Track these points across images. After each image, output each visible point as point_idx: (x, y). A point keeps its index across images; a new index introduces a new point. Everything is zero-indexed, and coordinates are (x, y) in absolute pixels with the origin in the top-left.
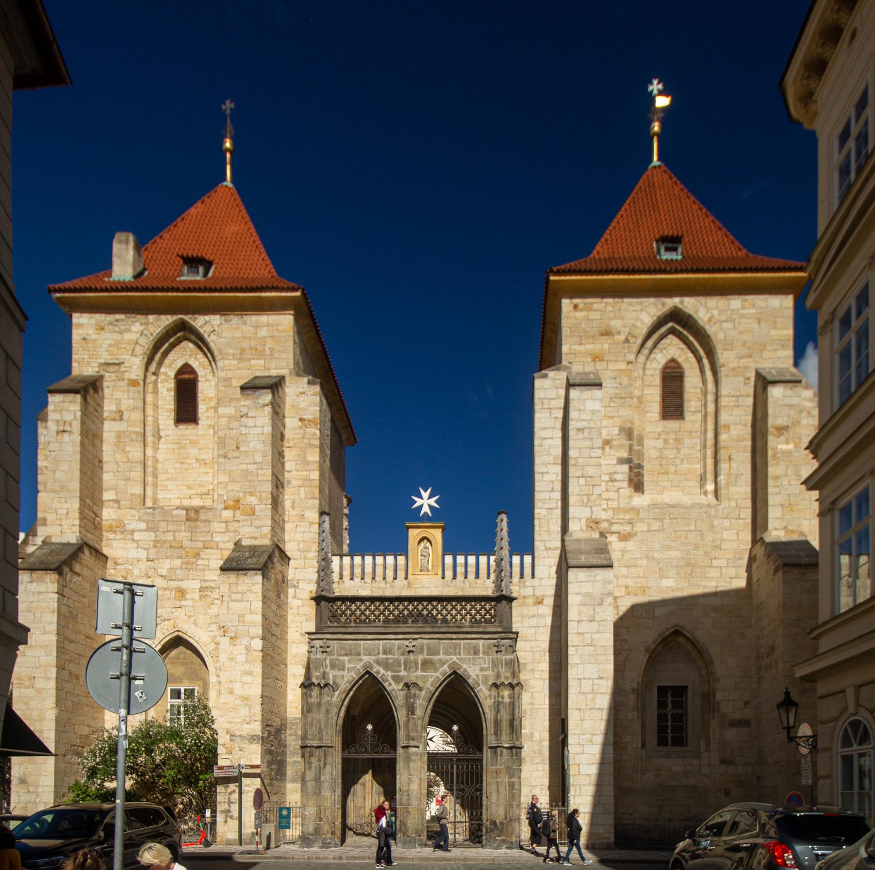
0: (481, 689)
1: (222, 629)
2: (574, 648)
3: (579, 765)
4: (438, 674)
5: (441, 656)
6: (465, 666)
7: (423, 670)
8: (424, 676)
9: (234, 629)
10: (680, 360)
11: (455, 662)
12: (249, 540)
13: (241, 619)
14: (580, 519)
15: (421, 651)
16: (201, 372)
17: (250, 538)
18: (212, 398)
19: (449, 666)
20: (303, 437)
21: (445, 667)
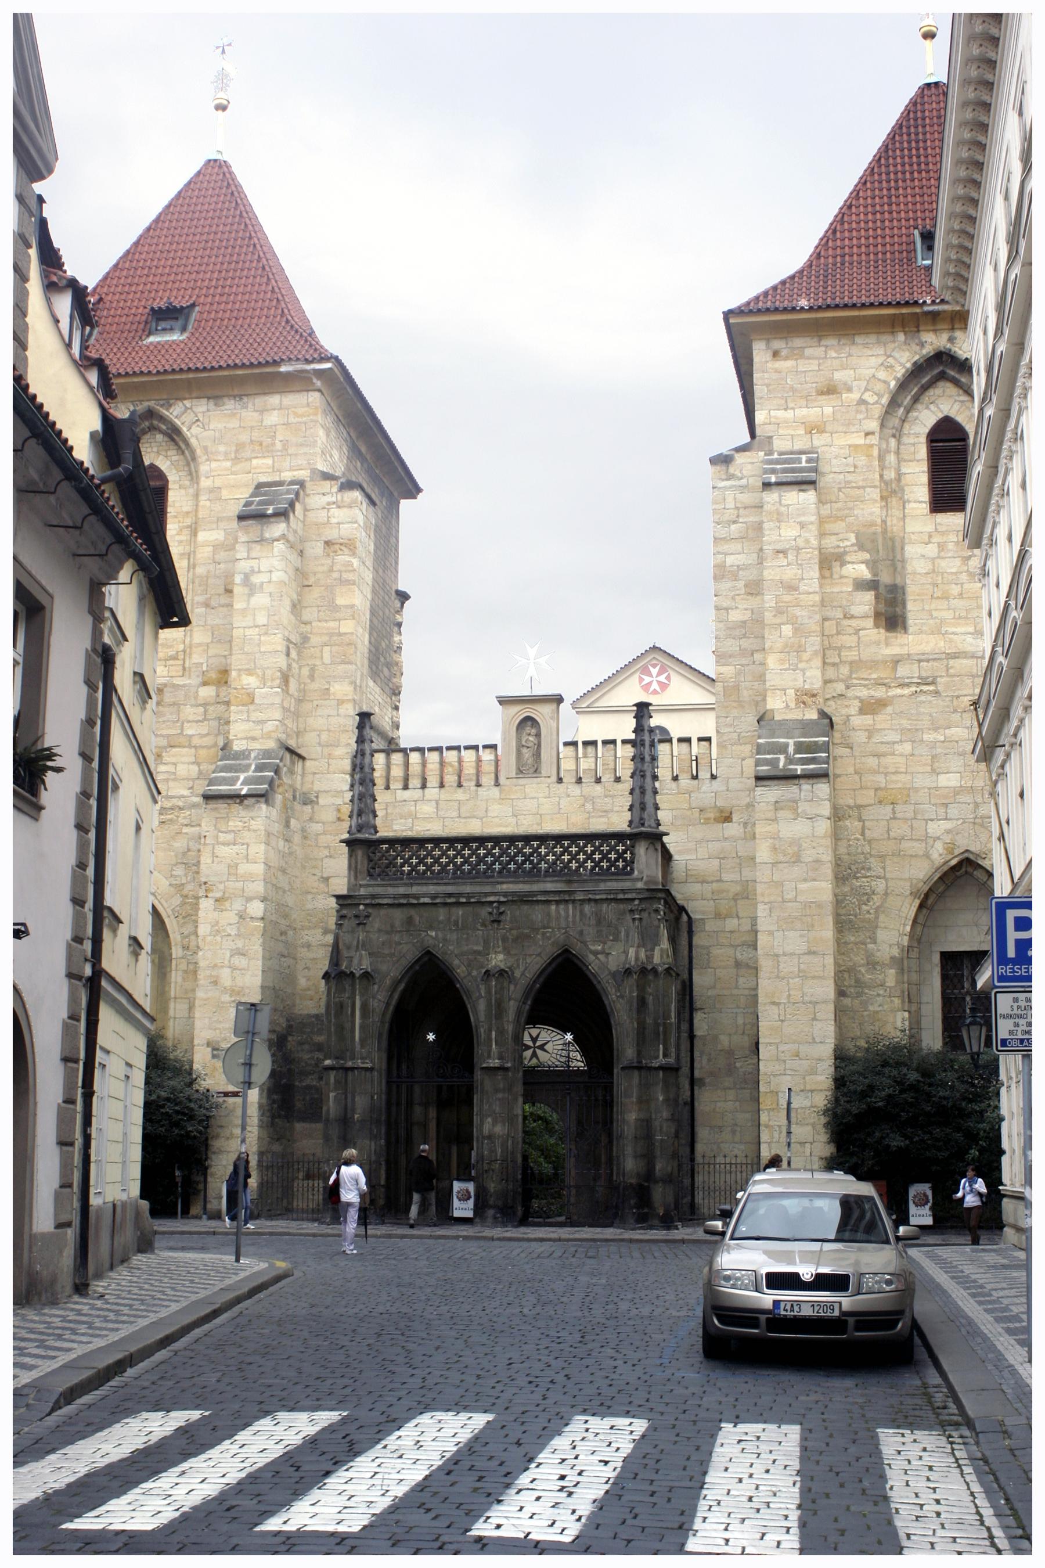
1: (203, 887)
3: (777, 1093)
9: (221, 887)
10: (959, 419)
12: (244, 742)
13: (233, 871)
14: (785, 690)
16: (172, 477)
17: (246, 738)
18: (188, 513)
20: (331, 570)
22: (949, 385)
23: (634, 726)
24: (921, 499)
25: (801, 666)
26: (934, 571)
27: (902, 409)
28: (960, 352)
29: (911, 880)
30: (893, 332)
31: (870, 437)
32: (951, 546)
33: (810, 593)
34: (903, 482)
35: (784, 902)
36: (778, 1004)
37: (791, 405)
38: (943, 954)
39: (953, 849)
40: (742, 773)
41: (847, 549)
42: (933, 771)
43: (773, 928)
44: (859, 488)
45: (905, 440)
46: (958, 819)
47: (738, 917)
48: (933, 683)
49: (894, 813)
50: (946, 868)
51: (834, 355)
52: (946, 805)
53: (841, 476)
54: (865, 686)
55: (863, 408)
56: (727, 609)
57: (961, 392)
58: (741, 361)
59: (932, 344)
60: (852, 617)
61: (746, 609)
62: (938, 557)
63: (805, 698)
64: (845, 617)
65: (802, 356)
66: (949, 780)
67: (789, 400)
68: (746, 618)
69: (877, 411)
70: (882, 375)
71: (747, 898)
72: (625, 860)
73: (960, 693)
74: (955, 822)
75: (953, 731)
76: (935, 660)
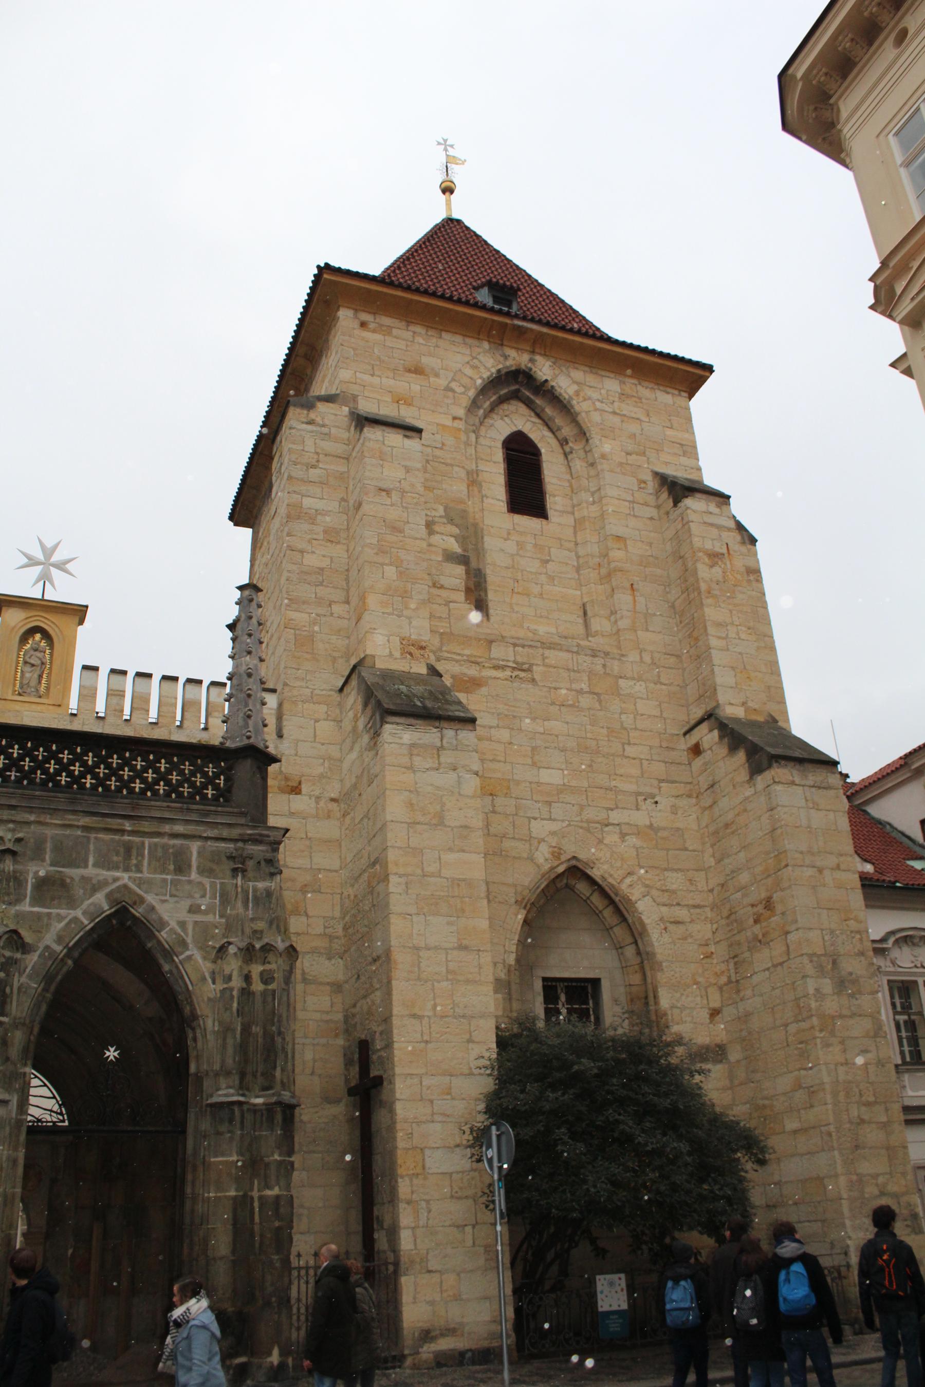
0: (189, 958)
2: (402, 880)
4: (78, 913)
6: (150, 898)
7: (36, 901)
8: (39, 916)
10: (533, 436)
11: (125, 886)
15: (38, 854)
19: (108, 896)
21: (100, 898)
23: (237, 613)
24: (498, 497)
25: (406, 613)
26: (513, 567)
27: (481, 412)
28: (540, 374)
29: (515, 886)
30: (479, 339)
31: (457, 421)
32: (529, 547)
33: (416, 539)
34: (480, 478)
35: (424, 876)
36: (419, 1017)
37: (377, 373)
38: (545, 979)
39: (560, 854)
40: (315, 736)
41: (436, 519)
42: (534, 764)
43: (412, 910)
44: (447, 464)
45: (482, 440)
46: (563, 821)
47: (307, 915)
48: (529, 670)
50: (553, 876)
51: (421, 341)
52: (549, 803)
53: (429, 450)
54: (457, 661)
55: (450, 394)
56: (302, 552)
57: (533, 414)
58: (301, 350)
59: (514, 359)
60: (442, 587)
61: (324, 556)
62: (518, 554)
63: (412, 649)
64: (434, 585)
66: (551, 777)
67: (375, 368)
68: (323, 565)
69: (465, 401)
70: (468, 371)
72: (216, 787)
74: (560, 823)
75: (553, 723)
76: (530, 646)
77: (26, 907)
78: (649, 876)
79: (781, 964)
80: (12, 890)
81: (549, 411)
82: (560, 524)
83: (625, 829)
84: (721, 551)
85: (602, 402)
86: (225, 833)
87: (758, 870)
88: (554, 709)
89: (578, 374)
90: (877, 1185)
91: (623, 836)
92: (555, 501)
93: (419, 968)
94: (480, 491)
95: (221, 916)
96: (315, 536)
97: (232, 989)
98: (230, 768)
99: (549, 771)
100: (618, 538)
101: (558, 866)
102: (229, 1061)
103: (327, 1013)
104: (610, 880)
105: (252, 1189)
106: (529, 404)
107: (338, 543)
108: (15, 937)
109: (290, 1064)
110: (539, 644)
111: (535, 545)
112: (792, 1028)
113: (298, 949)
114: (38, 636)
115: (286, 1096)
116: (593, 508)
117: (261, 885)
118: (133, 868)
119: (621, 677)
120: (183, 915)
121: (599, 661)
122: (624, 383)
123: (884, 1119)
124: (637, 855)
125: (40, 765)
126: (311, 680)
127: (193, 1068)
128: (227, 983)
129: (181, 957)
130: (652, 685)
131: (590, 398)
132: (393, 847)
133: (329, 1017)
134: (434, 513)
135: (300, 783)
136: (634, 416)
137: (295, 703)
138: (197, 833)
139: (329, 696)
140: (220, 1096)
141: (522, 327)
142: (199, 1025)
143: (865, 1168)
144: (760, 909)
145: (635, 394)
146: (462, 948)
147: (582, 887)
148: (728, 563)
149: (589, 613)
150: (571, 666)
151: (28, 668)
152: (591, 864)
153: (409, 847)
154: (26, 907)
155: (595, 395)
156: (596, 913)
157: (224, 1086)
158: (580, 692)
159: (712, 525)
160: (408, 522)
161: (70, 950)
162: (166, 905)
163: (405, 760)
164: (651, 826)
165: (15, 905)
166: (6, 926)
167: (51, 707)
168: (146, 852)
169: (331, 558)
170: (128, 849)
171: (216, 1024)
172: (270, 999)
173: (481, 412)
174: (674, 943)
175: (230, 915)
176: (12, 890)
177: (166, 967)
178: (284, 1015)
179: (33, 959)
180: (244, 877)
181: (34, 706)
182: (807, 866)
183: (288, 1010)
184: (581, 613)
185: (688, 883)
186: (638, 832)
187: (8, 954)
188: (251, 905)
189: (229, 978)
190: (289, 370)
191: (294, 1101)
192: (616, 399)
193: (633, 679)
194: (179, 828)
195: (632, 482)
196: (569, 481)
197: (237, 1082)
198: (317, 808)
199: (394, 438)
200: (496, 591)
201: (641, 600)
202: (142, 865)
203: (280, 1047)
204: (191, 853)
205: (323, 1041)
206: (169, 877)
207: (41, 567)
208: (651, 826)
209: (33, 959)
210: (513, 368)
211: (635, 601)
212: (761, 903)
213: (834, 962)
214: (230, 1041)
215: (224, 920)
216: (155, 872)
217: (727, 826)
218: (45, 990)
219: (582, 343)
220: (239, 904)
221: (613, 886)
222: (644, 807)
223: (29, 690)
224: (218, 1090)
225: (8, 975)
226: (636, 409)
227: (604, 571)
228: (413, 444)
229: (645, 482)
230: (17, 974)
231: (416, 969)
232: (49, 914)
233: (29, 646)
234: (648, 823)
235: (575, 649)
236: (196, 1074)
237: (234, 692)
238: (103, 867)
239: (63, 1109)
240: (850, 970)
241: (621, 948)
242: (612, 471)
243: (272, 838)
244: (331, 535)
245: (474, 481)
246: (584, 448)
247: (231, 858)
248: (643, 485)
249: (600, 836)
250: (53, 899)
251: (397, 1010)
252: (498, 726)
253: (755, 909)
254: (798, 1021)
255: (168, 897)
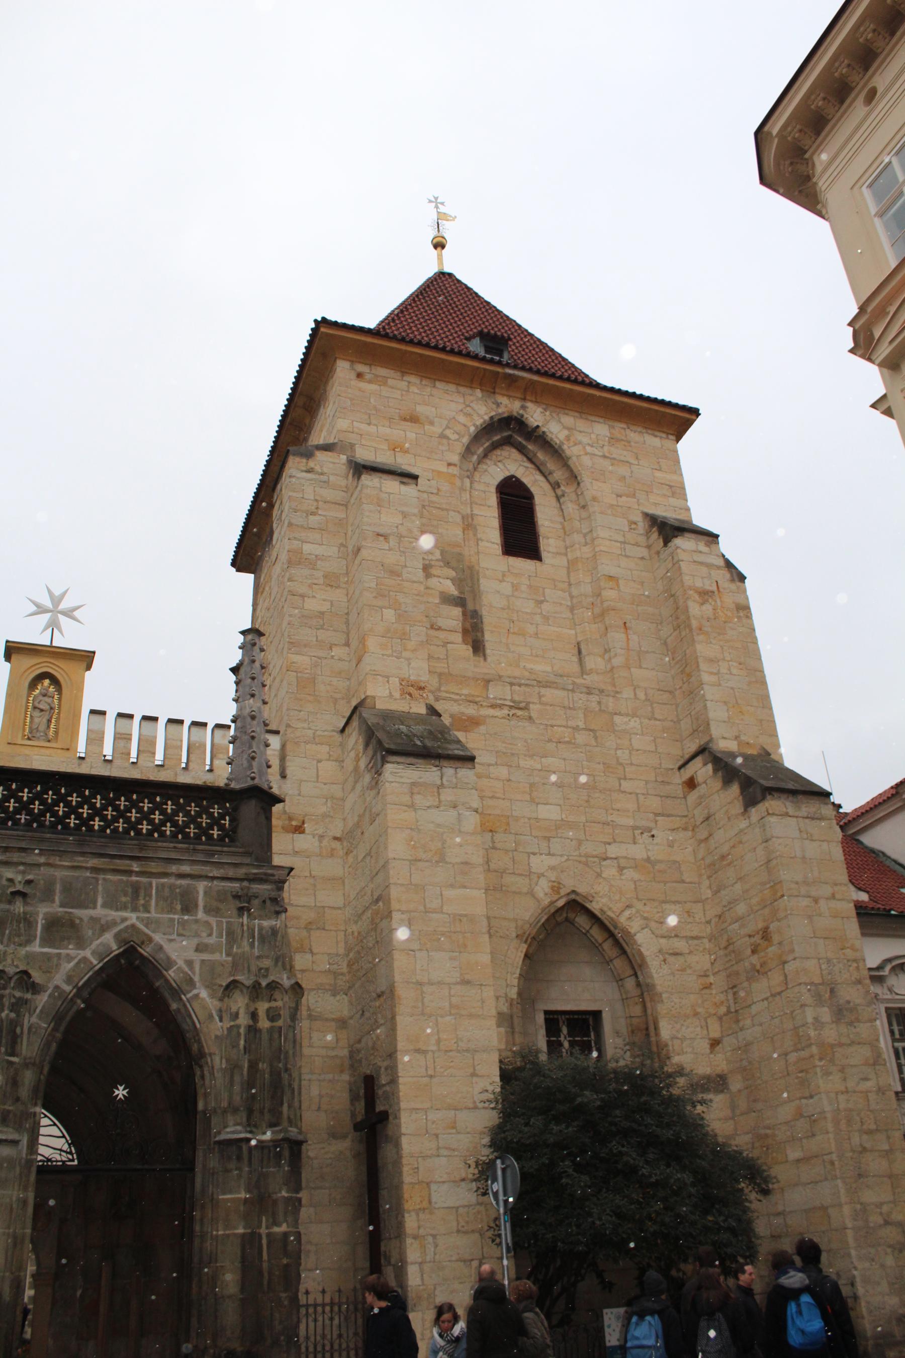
3: (428, 1184)
4: (87, 953)
5: (99, 911)
6: (158, 938)
7: (45, 942)
8: (48, 957)
10: (525, 480)
11: (133, 926)
14: (388, 677)
15: (48, 896)
19: (117, 936)
21: (108, 938)
22: (514, 450)
23: (240, 657)
24: (493, 540)
25: (404, 654)
26: (509, 608)
27: (475, 457)
28: (532, 419)
29: (516, 920)
30: (471, 387)
31: (452, 467)
33: (414, 582)
34: (475, 522)
35: (426, 912)
36: (425, 1052)
37: (374, 422)
38: (546, 1012)
39: (559, 888)
41: (433, 563)
42: (532, 800)
44: (442, 509)
45: (476, 485)
46: (562, 856)
47: (312, 952)
48: (526, 708)
49: (493, 842)
50: (553, 910)
51: (416, 391)
52: (548, 839)
53: (425, 495)
54: (455, 701)
55: (445, 441)
56: (302, 596)
57: (525, 459)
60: (439, 629)
61: (324, 600)
62: (513, 596)
63: (411, 690)
64: (432, 627)
65: (385, 384)
66: (550, 813)
67: (372, 417)
68: (324, 609)
69: (459, 448)
70: (462, 419)
71: (324, 929)
72: (221, 828)
73: (554, 722)
74: (559, 858)
76: (526, 685)
77: (36, 947)
78: (647, 908)
79: (779, 993)
80: (22, 931)
81: (541, 456)
82: (553, 566)
83: (623, 862)
84: (711, 589)
85: (592, 446)
86: (231, 873)
87: (754, 901)
88: (551, 746)
89: (568, 420)
90: (881, 1214)
91: (621, 869)
92: (548, 543)
93: (423, 1003)
94: (475, 535)
95: (228, 955)
96: (316, 581)
97: (238, 1027)
98: (235, 809)
99: (548, 807)
100: (611, 578)
101: (557, 900)
102: (237, 1099)
103: (333, 1049)
104: (610, 913)
105: (260, 1227)
106: (521, 449)
107: (338, 587)
108: (25, 977)
109: (296, 1100)
110: (535, 683)
111: (530, 587)
112: (793, 1057)
113: (304, 986)
114: (47, 682)
115: (293, 1132)
116: (586, 549)
117: (266, 923)
118: (141, 908)
119: (616, 714)
120: (192, 955)
121: (594, 698)
122: (613, 427)
123: (887, 1147)
124: (636, 888)
125: (50, 808)
126: (312, 722)
127: (201, 1106)
128: (234, 1020)
129: (189, 996)
130: (647, 720)
131: (580, 443)
132: (395, 884)
133: (333, 1053)
134: (430, 557)
135: (303, 823)
136: (623, 458)
137: (297, 743)
138: (204, 873)
139: (331, 737)
140: (228, 1133)
141: (513, 375)
142: (207, 1063)
143: (869, 1196)
144: (757, 939)
145: (623, 438)
146: (466, 982)
147: (582, 921)
148: (718, 601)
149: (584, 651)
150: (566, 704)
151: (37, 714)
152: (589, 898)
153: (411, 884)
154: (36, 947)
155: (585, 440)
156: (595, 947)
157: (231, 1123)
158: (576, 729)
159: (701, 563)
160: (406, 566)
161: (80, 989)
162: (173, 944)
163: (406, 799)
164: (648, 860)
165: (25, 946)
166: (17, 967)
167: (59, 751)
168: (154, 892)
169: (332, 602)
170: (136, 889)
171: (224, 1061)
172: (276, 1036)
173: (475, 458)
174: (673, 974)
175: (237, 953)
176: (22, 931)
177: (174, 1006)
178: (291, 1052)
179: (42, 1000)
180: (249, 915)
181: (43, 750)
182: (804, 896)
183: (294, 1047)
184: (576, 651)
185: (686, 915)
186: (636, 865)
187: (18, 994)
188: (256, 943)
189: (236, 1016)
190: (288, 420)
191: (300, 1138)
192: (606, 444)
193: (627, 715)
194: (186, 869)
195: (623, 524)
196: (561, 523)
197: (244, 1119)
198: (321, 847)
199: (391, 485)
200: (492, 632)
201: (634, 638)
202: (150, 905)
203: (286, 1083)
204: (198, 893)
205: (330, 1076)
206: (176, 917)
207: (49, 615)
208: (648, 860)
209: (42, 1000)
210: (506, 415)
211: (628, 639)
212: (758, 933)
213: (832, 991)
214: (237, 1078)
215: (230, 959)
216: (162, 912)
217: (723, 857)
218: (55, 1029)
219: (571, 390)
220: (245, 943)
221: (612, 919)
222: (641, 841)
223: (38, 735)
224: (225, 1127)
225: (18, 1016)
226: (625, 453)
227: (597, 610)
228: (409, 491)
229: (635, 523)
230: (27, 1015)
231: (420, 1004)
232: (59, 955)
233: (38, 691)
234: (645, 857)
235: (570, 687)
236: (204, 1112)
237: (238, 735)
238: (111, 908)
239: (73, 1149)
240: (848, 998)
241: (621, 980)
242: (602, 513)
243: (276, 877)
244: (331, 581)
245: (469, 524)
246: (575, 491)
247: (237, 897)
248: (633, 526)
249: (598, 870)
250: (63, 939)
251: (401, 1045)
252: (496, 764)
253: (753, 940)
254: (797, 1050)
255: (175, 936)
